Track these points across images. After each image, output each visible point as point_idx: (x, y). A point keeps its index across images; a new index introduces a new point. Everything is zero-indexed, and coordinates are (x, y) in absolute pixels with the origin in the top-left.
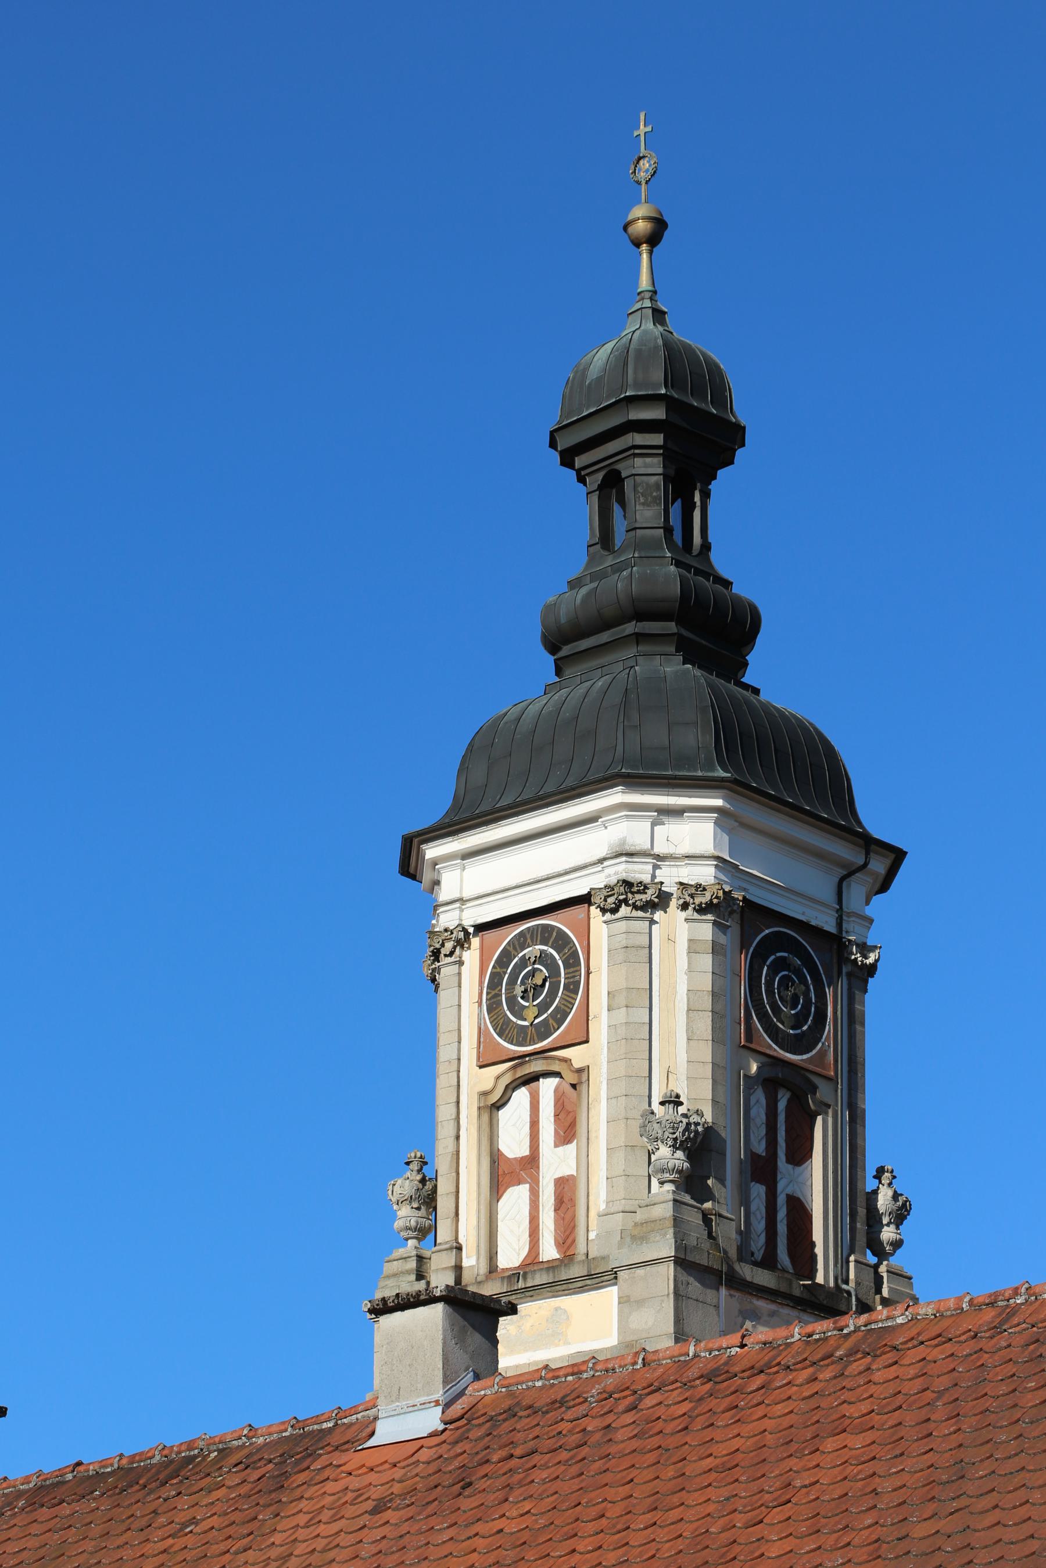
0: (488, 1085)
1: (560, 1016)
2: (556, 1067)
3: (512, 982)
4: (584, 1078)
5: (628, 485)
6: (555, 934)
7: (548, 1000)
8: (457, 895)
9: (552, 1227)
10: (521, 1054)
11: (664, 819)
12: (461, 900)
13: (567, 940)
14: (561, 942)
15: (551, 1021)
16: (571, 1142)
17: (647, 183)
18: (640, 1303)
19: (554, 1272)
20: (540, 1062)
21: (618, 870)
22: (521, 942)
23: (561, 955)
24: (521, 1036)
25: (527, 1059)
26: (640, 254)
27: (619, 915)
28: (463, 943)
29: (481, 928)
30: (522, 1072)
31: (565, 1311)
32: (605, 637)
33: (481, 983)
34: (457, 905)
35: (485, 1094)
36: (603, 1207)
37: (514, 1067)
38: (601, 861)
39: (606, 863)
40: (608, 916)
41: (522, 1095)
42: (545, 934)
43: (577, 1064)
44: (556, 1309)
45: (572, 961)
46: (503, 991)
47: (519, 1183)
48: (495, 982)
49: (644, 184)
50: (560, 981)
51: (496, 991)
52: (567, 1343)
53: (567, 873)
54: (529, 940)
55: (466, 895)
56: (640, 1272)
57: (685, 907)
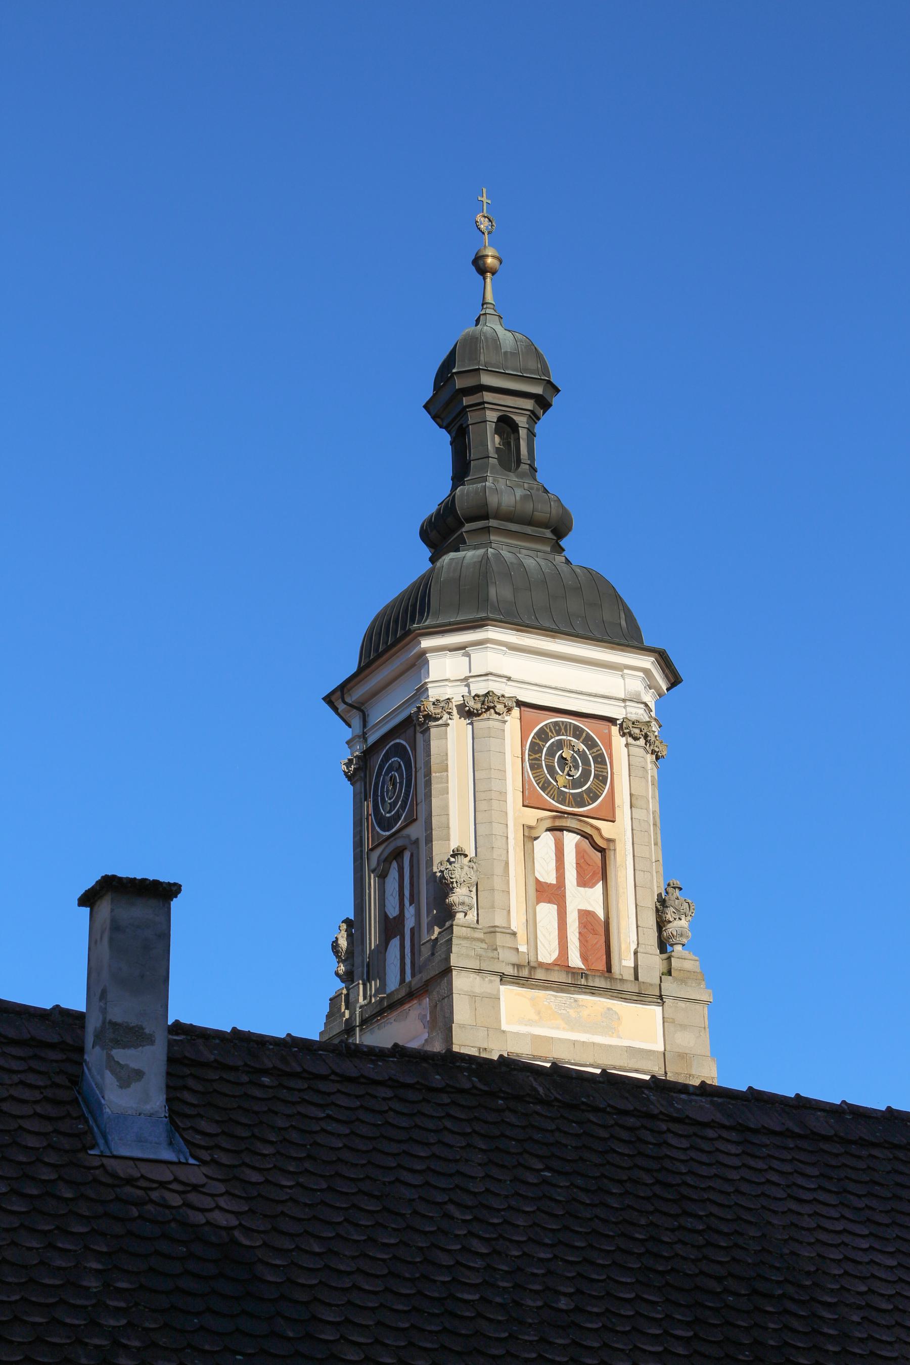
0: (533, 823)
2: (588, 830)
3: (551, 753)
6: (584, 735)
7: (582, 780)
8: (508, 675)
9: (577, 943)
10: (564, 811)
12: (509, 679)
14: (590, 743)
15: (585, 796)
17: (489, 233)
18: (683, 1027)
19: (611, 982)
22: (558, 728)
23: (591, 752)
24: (561, 797)
25: (566, 816)
26: (485, 279)
27: (638, 743)
28: (509, 710)
30: (558, 823)
31: (616, 1013)
32: (529, 530)
34: (504, 680)
36: (633, 947)
37: (555, 817)
38: (624, 700)
39: (628, 703)
40: (630, 740)
42: (577, 732)
43: (606, 834)
44: (609, 1009)
45: (600, 760)
46: (543, 758)
47: (550, 902)
48: (535, 749)
49: (486, 234)
51: (537, 756)
52: (619, 1037)
53: (596, 696)
55: (513, 677)
56: (682, 1004)
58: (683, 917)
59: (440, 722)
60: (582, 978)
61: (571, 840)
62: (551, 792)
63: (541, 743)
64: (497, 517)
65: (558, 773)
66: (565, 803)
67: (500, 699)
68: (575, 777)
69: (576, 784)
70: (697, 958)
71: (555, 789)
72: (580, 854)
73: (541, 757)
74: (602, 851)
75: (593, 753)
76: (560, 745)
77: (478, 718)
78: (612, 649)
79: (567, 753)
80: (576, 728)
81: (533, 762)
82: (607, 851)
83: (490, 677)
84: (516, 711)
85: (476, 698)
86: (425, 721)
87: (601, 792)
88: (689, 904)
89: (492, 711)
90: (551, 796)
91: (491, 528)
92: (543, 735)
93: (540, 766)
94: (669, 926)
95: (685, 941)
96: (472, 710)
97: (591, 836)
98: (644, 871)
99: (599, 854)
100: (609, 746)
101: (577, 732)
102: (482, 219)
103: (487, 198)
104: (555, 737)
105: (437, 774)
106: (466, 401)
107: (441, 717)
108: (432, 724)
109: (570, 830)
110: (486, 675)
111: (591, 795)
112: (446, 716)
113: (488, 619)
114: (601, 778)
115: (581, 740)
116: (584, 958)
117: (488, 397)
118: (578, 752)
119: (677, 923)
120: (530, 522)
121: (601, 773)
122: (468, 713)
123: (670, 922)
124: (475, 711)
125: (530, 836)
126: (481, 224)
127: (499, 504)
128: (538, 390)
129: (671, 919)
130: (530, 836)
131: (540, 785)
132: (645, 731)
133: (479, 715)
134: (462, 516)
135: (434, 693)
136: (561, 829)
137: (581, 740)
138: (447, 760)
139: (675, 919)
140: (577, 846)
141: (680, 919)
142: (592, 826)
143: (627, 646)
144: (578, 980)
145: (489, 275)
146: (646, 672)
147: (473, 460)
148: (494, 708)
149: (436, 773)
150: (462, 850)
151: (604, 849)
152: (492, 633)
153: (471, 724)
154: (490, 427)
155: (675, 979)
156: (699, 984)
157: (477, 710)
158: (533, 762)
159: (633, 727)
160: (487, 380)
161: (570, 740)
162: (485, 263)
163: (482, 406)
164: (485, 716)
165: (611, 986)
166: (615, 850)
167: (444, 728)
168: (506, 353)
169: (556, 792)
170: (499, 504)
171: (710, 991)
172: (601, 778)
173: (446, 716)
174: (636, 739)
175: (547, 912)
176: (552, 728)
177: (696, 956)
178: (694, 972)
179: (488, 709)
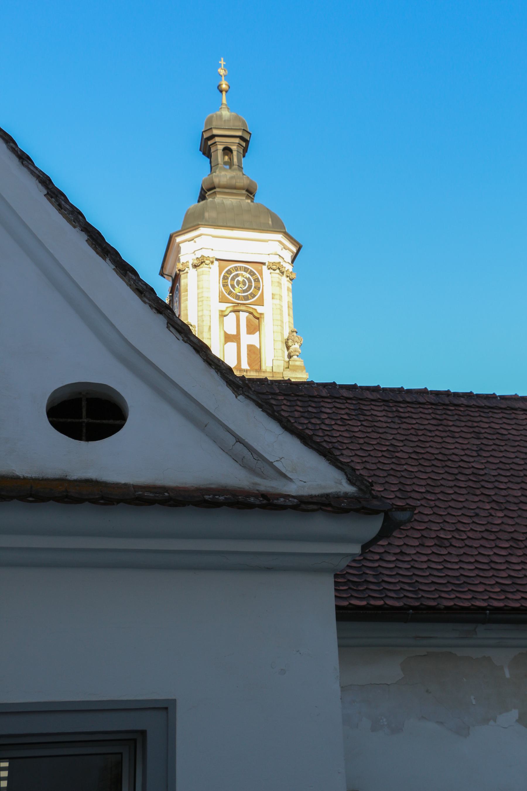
0: (224, 309)
1: (253, 295)
2: (251, 310)
3: (233, 279)
4: (262, 316)
5: (235, 153)
6: (249, 270)
11: (283, 249)
13: (254, 274)
14: (252, 273)
16: (254, 334)
17: (225, 76)
20: (245, 307)
21: (277, 259)
22: (236, 269)
23: (253, 277)
25: (240, 305)
26: (222, 94)
27: (275, 272)
28: (212, 262)
29: (217, 260)
30: (236, 308)
33: (220, 277)
35: (222, 311)
37: (234, 306)
40: (272, 271)
41: (233, 315)
43: (259, 311)
45: (257, 280)
47: (233, 341)
48: (225, 278)
49: (223, 76)
50: (252, 286)
54: (239, 269)
57: (287, 276)
58: (296, 343)
59: (185, 272)
60: (244, 372)
61: (243, 316)
62: (233, 295)
63: (228, 275)
64: (219, 187)
65: (236, 287)
66: (239, 299)
67: (207, 258)
68: (243, 289)
69: (244, 291)
70: (302, 360)
71: (234, 294)
72: (248, 321)
73: (228, 281)
74: (258, 319)
75: (254, 278)
76: (237, 275)
77: (199, 267)
78: (261, 232)
79: (240, 279)
80: (245, 268)
81: (224, 283)
82: (260, 318)
83: (203, 249)
84: (216, 263)
85: (197, 259)
86: (179, 272)
87: (257, 294)
88: (299, 338)
89: (204, 263)
90: (232, 297)
91: (216, 192)
92: (229, 272)
93: (227, 285)
94: (291, 347)
95: (297, 354)
96: (195, 264)
97: (252, 313)
98: (278, 326)
99: (257, 320)
100: (261, 274)
101: (246, 270)
102: (221, 71)
103: (224, 61)
104: (235, 272)
105: (184, 294)
106: (209, 143)
107: (185, 270)
108: (181, 273)
109: (243, 311)
110: (201, 249)
111: (252, 295)
112: (187, 269)
113: (199, 225)
114: (257, 288)
115: (248, 272)
116: (249, 364)
117: (217, 139)
118: (246, 278)
119: (293, 347)
120: (235, 188)
121: (257, 286)
122: (195, 266)
123: (290, 346)
124: (197, 265)
125: (223, 315)
126: (221, 72)
127: (219, 182)
128: (239, 133)
129: (291, 345)
130: (223, 315)
131: (227, 293)
132: (278, 266)
133: (199, 266)
134: (206, 189)
135: (183, 259)
136: (239, 311)
137: (248, 272)
138: (187, 287)
139: (292, 345)
140: (247, 318)
141: (295, 344)
142: (253, 308)
143: (267, 230)
144: (242, 373)
145: (224, 93)
146: (280, 242)
147: (214, 166)
148: (204, 262)
149: (183, 293)
150: (189, 323)
151: (259, 318)
152: (202, 230)
153: (196, 270)
154: (220, 153)
155: (291, 370)
156: (303, 371)
157: (197, 264)
158: (224, 283)
159: (272, 265)
160: (216, 132)
161: (242, 274)
162: (221, 88)
163: (215, 144)
164: (201, 266)
165: (259, 374)
166: (264, 318)
167: (186, 274)
168: (225, 121)
169: (235, 295)
170: (219, 182)
171: (307, 373)
172: (257, 288)
173: (187, 269)
174: (274, 270)
175: (232, 346)
176: (234, 269)
177: (302, 359)
178: (300, 366)
179: (202, 263)
